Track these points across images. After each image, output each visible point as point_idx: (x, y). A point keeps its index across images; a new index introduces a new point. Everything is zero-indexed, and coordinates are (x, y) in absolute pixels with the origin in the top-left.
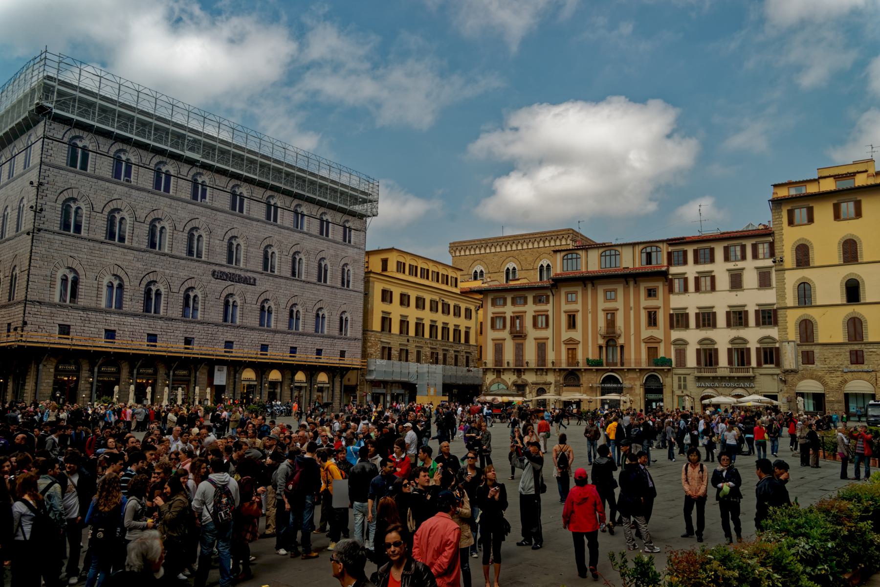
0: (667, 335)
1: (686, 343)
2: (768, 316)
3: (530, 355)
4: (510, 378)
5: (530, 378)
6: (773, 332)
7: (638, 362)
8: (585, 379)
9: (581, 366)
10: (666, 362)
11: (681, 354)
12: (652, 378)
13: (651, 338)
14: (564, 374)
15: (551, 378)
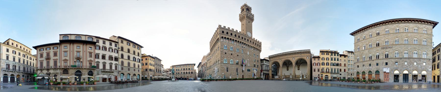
0: (94, 60)
1: (99, 62)
2: (116, 59)
3: (52, 64)
4: (45, 72)
5: (51, 71)
6: (117, 62)
7: (86, 66)
8: (71, 71)
9: (68, 67)
10: (94, 67)
11: (98, 65)
12: (91, 72)
13: (91, 60)
14: (63, 70)
15: (58, 71)
